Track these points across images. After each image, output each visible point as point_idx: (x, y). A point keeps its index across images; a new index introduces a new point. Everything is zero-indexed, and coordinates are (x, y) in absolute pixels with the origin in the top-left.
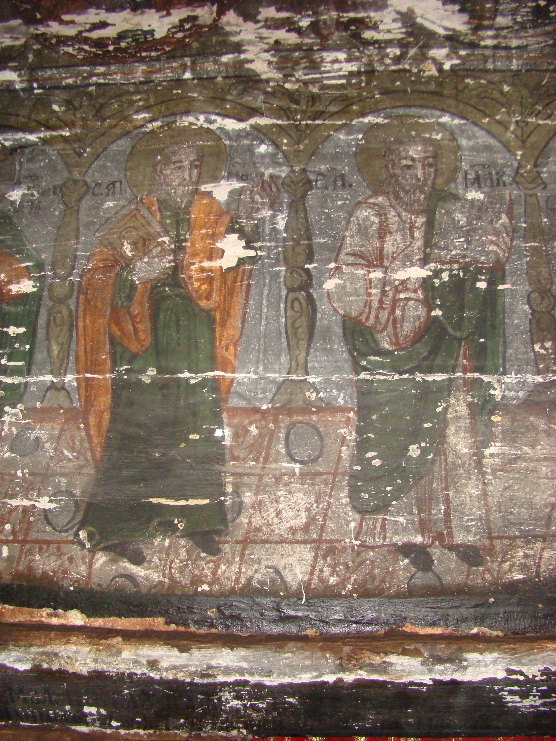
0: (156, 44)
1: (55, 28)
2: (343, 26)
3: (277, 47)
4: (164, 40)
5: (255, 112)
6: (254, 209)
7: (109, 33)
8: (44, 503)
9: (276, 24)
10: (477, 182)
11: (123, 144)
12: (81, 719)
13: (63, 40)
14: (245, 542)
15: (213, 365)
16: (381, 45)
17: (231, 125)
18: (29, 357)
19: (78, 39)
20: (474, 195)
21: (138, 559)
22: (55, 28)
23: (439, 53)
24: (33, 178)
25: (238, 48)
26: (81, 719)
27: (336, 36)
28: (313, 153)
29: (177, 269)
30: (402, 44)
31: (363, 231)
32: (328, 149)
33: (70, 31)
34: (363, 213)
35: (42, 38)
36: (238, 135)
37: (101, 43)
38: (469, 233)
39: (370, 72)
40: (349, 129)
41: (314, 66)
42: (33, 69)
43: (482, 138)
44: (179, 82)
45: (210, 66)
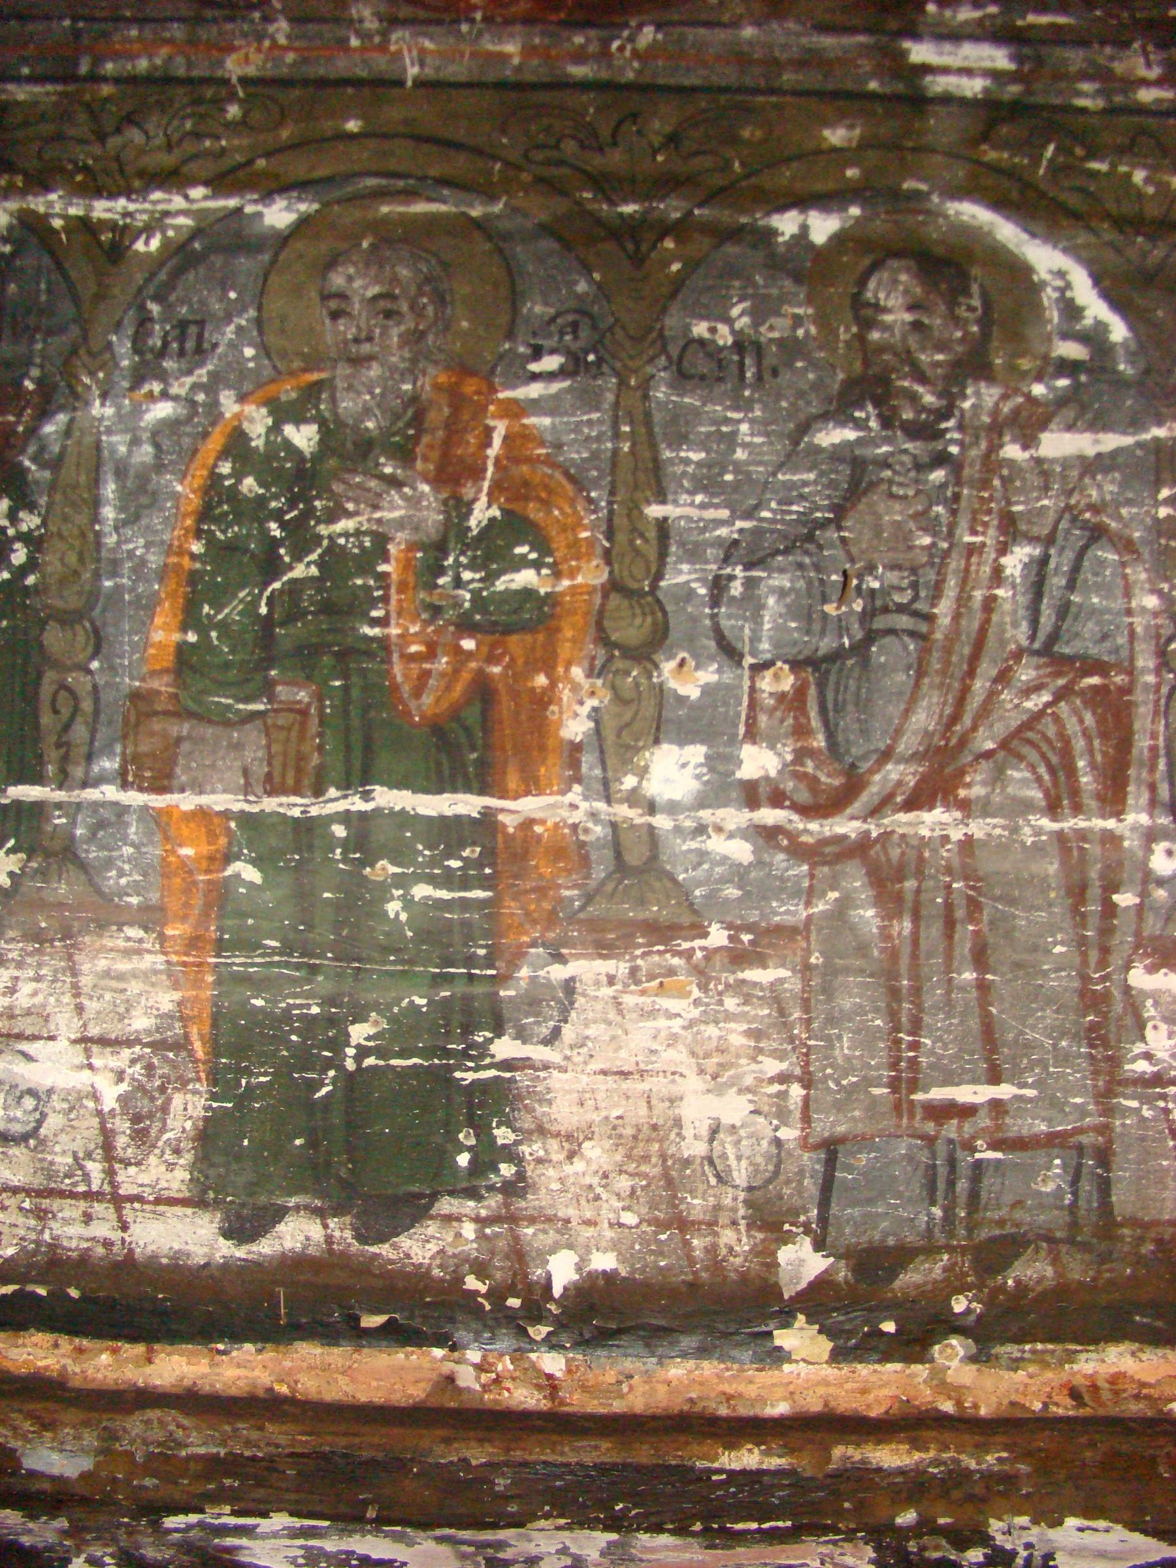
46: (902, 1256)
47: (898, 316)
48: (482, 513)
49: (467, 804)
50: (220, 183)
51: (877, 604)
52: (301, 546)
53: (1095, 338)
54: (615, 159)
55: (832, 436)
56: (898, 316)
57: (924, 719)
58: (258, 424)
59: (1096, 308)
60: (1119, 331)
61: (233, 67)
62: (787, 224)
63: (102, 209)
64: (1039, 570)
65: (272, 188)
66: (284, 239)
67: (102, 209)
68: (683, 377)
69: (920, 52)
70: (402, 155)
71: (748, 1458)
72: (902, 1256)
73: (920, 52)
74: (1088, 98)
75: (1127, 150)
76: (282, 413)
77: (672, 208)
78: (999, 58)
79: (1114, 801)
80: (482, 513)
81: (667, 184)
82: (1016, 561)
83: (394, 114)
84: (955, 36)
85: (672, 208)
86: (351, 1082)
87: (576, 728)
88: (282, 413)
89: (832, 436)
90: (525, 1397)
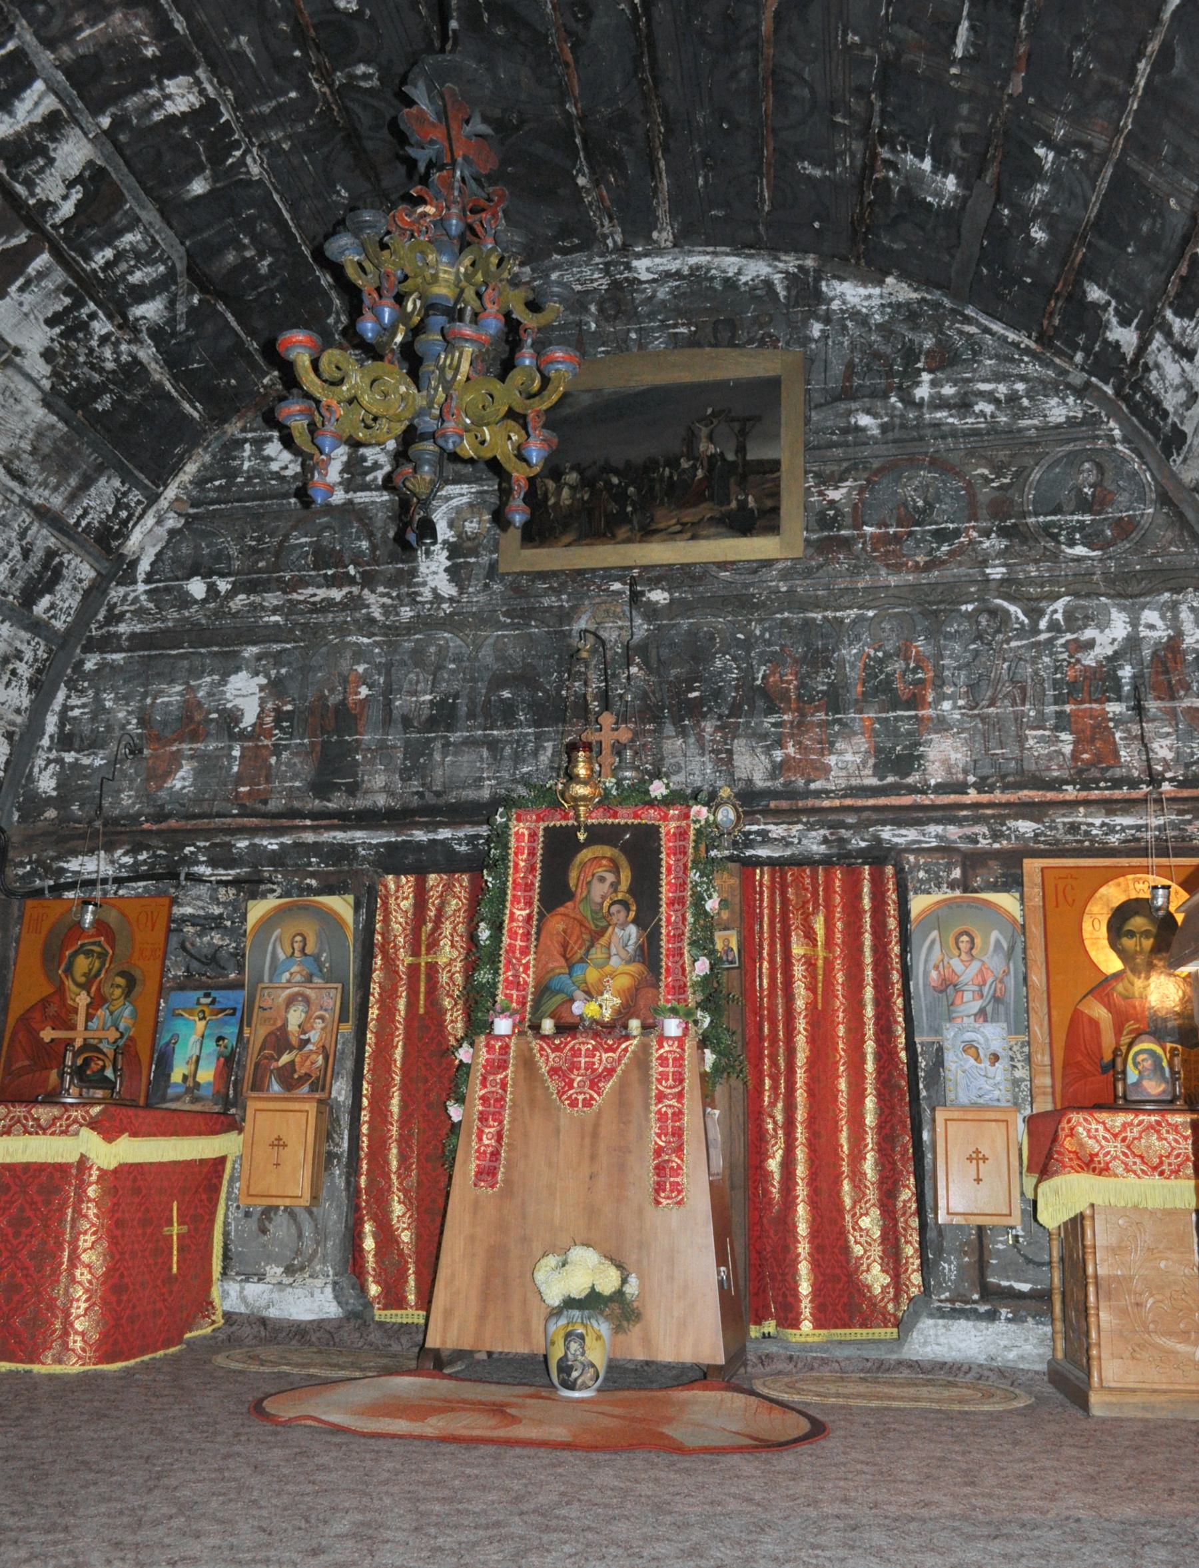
0: (336, 604)
1: (295, 596)
2: (409, 595)
3: (383, 606)
4: (341, 602)
5: (374, 635)
6: (372, 676)
7: (317, 599)
8: (297, 784)
9: (383, 595)
10: (454, 661)
11: (324, 649)
12: (310, 864)
13: (300, 602)
14: (366, 792)
15: (357, 733)
16: (423, 603)
17: (366, 640)
18: (291, 734)
19: (305, 601)
20: (452, 666)
21: (329, 801)
22: (295, 596)
23: (445, 606)
24: (289, 664)
25: (368, 606)
26: (310, 864)
27: (407, 600)
28: (395, 651)
29: (345, 699)
30: (431, 603)
31: (410, 682)
32: (400, 650)
33: (301, 598)
34: (412, 676)
35: (290, 601)
36: (368, 645)
37: (314, 604)
38: (448, 681)
39: (418, 616)
40: (409, 641)
41: (397, 614)
42: (287, 615)
43: (459, 642)
44: (346, 622)
45: (358, 615)
46: (987, 778)
47: (984, 623)
48: (912, 665)
49: (912, 713)
50: (860, 608)
51: (981, 675)
52: (881, 672)
53: (1022, 623)
54: (931, 598)
55: (973, 647)
56: (984, 623)
57: (989, 693)
58: (872, 652)
59: (1022, 617)
60: (1026, 621)
61: (860, 585)
62: (963, 608)
63: (838, 614)
64: (1009, 668)
65: (869, 609)
66: (872, 618)
67: (838, 614)
68: (945, 639)
69: (988, 571)
70: (892, 600)
71: (965, 813)
72: (987, 778)
73: (988, 571)
74: (1021, 576)
75: (1030, 585)
76: (876, 650)
77: (942, 607)
78: (1004, 570)
79: (1023, 704)
80: (912, 665)
81: (941, 602)
82: (1005, 665)
83: (890, 592)
84: (995, 566)
85: (942, 607)
86: (898, 756)
87: (930, 699)
88: (876, 650)
89: (973, 647)
90: (928, 802)
